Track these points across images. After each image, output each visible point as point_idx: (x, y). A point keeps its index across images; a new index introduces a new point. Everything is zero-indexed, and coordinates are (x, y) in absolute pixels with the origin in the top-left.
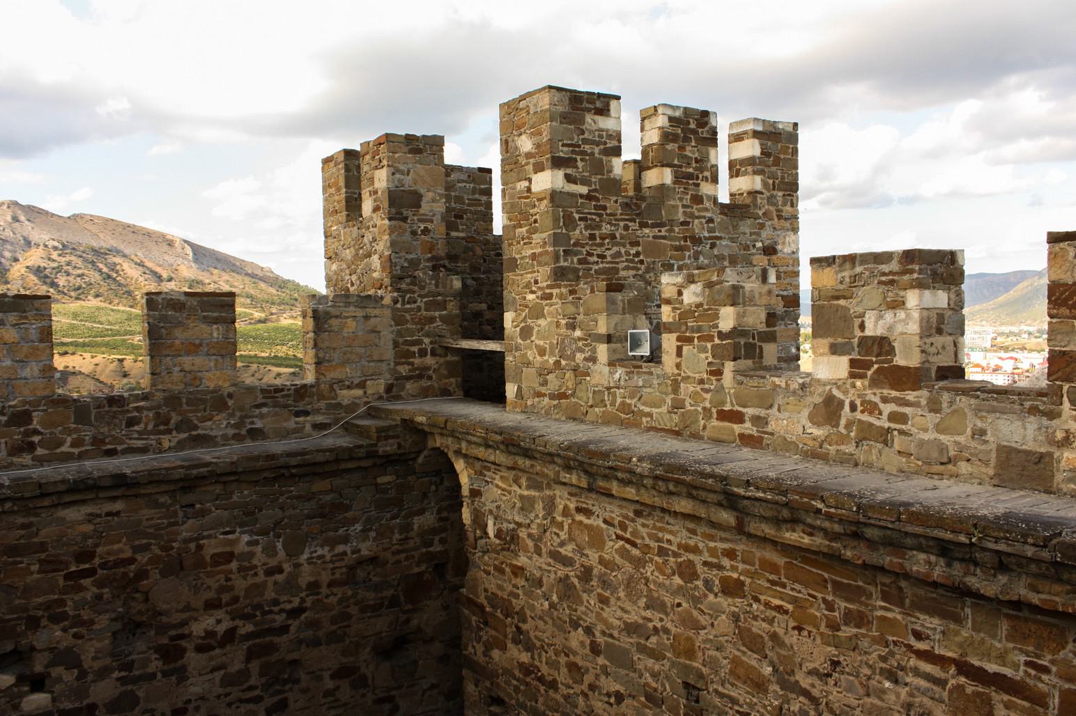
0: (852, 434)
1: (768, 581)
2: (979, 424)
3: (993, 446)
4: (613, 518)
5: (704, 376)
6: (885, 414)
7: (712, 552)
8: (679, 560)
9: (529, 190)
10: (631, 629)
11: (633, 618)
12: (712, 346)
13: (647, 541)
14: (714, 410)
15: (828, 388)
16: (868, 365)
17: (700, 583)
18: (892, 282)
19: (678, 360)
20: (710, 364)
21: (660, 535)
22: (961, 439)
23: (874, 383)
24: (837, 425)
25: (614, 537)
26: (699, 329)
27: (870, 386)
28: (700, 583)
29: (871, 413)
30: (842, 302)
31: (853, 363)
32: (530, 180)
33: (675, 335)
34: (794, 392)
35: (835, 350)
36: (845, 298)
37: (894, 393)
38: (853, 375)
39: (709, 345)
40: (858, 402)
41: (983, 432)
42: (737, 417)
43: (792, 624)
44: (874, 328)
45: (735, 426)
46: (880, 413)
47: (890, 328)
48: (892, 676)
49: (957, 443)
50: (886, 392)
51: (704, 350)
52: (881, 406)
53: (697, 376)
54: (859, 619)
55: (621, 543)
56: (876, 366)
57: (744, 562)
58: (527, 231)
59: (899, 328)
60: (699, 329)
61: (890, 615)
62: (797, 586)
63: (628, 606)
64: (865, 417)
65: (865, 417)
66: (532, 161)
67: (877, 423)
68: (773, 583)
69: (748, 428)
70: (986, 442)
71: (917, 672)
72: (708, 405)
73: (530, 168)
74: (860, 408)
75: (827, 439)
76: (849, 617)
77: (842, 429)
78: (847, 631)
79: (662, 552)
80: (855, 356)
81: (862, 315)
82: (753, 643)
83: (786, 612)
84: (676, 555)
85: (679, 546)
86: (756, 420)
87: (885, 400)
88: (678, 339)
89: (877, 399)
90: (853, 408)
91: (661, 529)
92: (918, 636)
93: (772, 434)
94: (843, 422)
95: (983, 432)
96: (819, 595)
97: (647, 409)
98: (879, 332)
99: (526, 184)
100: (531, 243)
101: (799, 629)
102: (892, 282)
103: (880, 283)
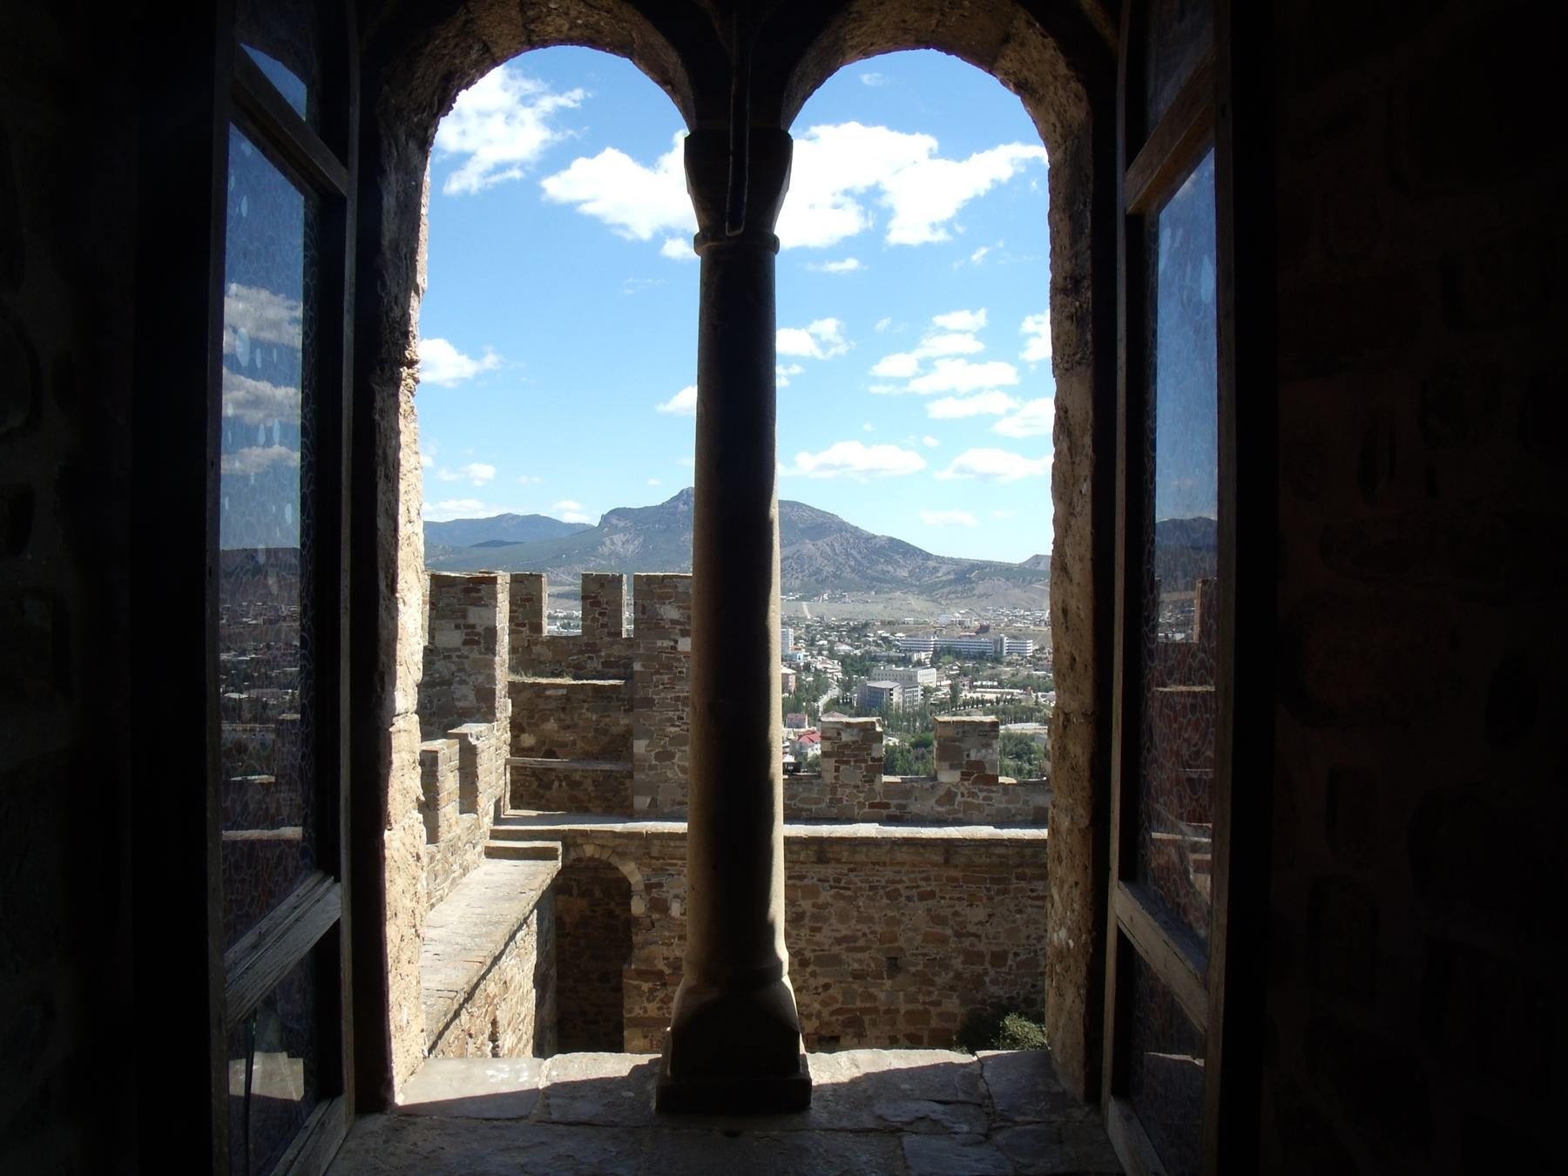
0: (962, 808)
1: (952, 886)
2: (1026, 798)
3: (1031, 807)
4: (828, 877)
5: (860, 783)
6: (981, 798)
7: (912, 881)
8: (888, 890)
9: (674, 648)
10: (839, 941)
11: (845, 932)
12: (866, 766)
13: (859, 884)
14: (867, 803)
15: (948, 786)
16: (972, 774)
17: (903, 899)
18: (986, 735)
19: (836, 774)
20: (864, 776)
21: (871, 879)
22: (1018, 806)
23: (975, 783)
24: (954, 804)
25: (829, 888)
26: (855, 756)
27: (972, 784)
28: (903, 899)
29: (973, 797)
30: (957, 744)
31: (963, 774)
32: (676, 642)
33: (834, 760)
34: (927, 789)
35: (952, 767)
36: (959, 741)
37: (985, 787)
38: (962, 779)
39: (863, 765)
40: (966, 793)
41: (1028, 801)
42: (886, 806)
43: (966, 903)
44: (974, 756)
45: (883, 811)
46: (978, 797)
47: (985, 757)
48: (1020, 912)
49: (1016, 808)
50: (981, 787)
51: (860, 768)
52: (979, 794)
53: (852, 783)
54: (1005, 892)
55: (836, 890)
56: (976, 775)
57: (935, 880)
58: (669, 679)
59: (989, 757)
60: (855, 756)
61: (1019, 885)
62: (970, 885)
63: (839, 926)
64: (970, 799)
65: (970, 799)
66: (679, 627)
67: (976, 802)
68: (956, 887)
69: (892, 811)
70: (1029, 806)
71: (1031, 906)
72: (862, 800)
73: (677, 631)
74: (966, 795)
75: (948, 813)
76: (998, 892)
77: (956, 807)
78: (997, 899)
79: (872, 888)
80: (964, 770)
81: (969, 750)
82: (940, 920)
83: (964, 899)
84: (883, 888)
85: (887, 882)
86: (899, 807)
87: (981, 791)
88: (836, 762)
89: (976, 790)
90: (963, 795)
91: (873, 875)
92: (1032, 891)
93: (910, 813)
94: (956, 803)
95: (1028, 801)
96: (983, 886)
97: (806, 806)
98: (978, 759)
99: (672, 643)
100: (674, 688)
101: (971, 905)
102: (986, 735)
103: (979, 735)
